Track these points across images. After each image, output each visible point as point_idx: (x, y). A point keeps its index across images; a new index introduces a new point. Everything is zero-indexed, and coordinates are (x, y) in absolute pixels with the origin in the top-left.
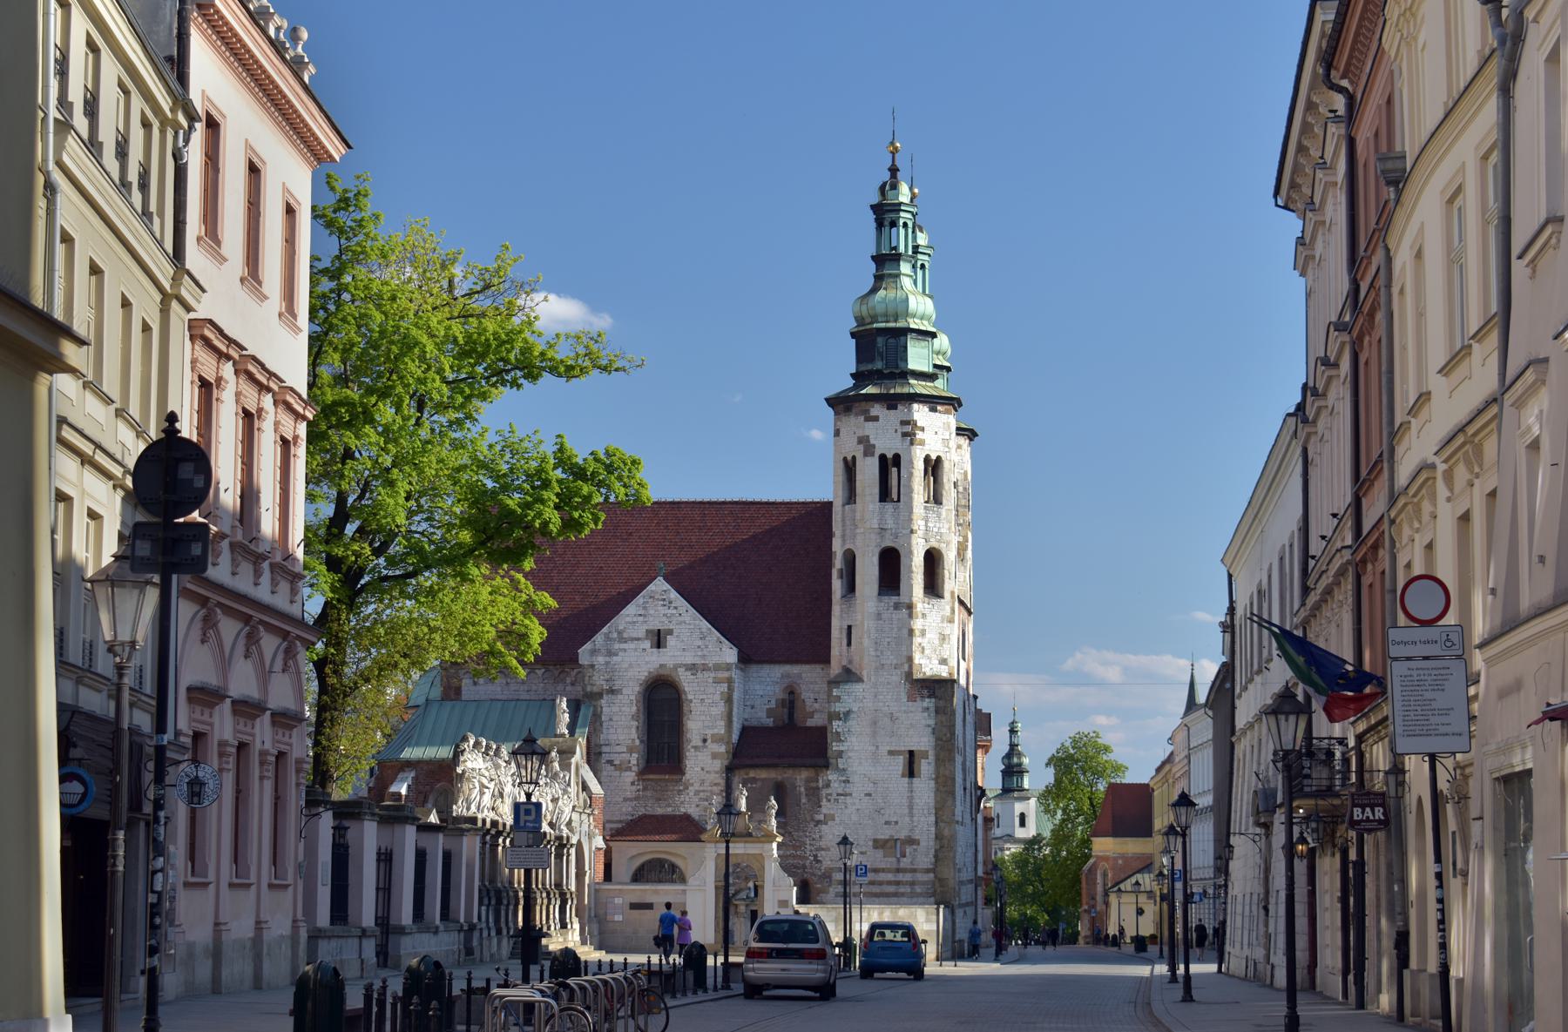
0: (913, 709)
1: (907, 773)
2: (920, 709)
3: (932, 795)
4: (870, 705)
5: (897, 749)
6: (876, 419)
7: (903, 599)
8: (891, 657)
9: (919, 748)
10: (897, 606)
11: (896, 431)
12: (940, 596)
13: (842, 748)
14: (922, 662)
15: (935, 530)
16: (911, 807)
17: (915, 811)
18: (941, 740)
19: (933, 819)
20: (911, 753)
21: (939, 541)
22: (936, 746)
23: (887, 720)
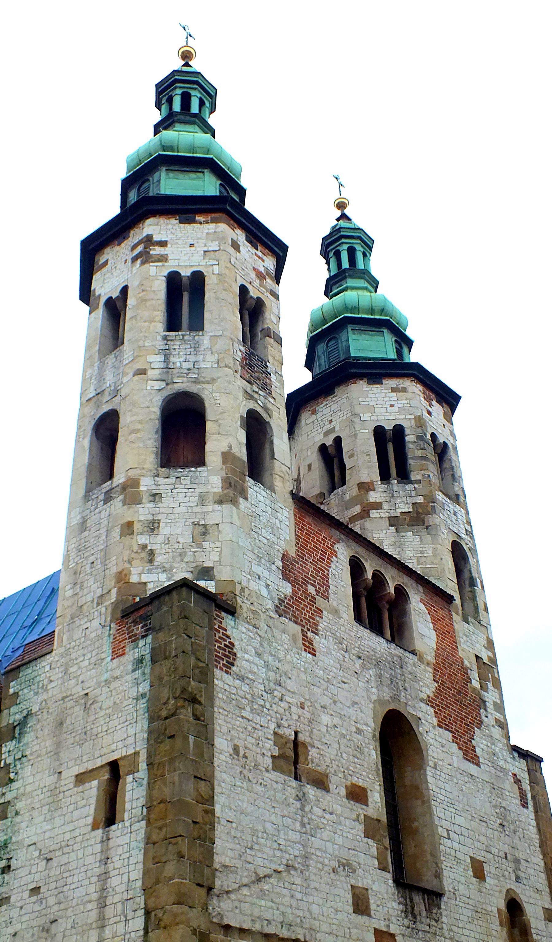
0: (117, 673)
1: (102, 817)
2: (130, 667)
3: (141, 857)
4: (55, 691)
5: (90, 766)
6: (106, 263)
7: (119, 478)
8: (94, 587)
9: (124, 754)
10: (108, 498)
11: (126, 260)
12: (201, 462)
13: (9, 797)
14: (145, 578)
15: (185, 365)
16: (102, 904)
17: (109, 911)
18: (159, 718)
19: (139, 923)
20: (114, 766)
21: (196, 381)
22: (150, 733)
23: (78, 710)
